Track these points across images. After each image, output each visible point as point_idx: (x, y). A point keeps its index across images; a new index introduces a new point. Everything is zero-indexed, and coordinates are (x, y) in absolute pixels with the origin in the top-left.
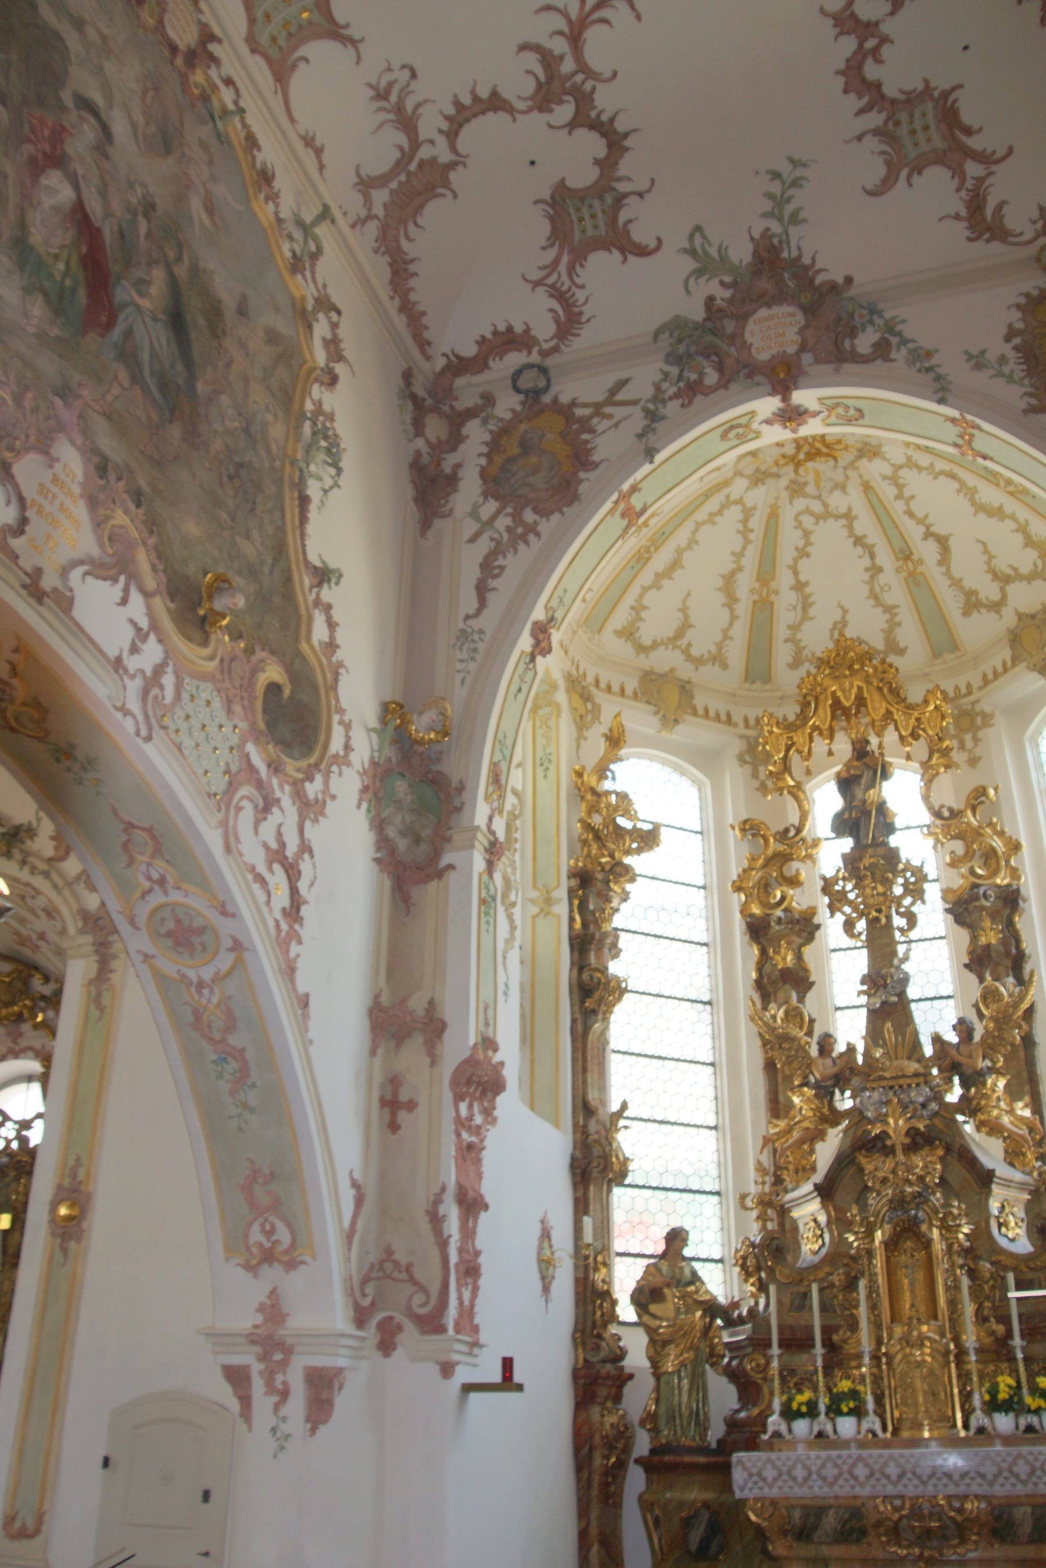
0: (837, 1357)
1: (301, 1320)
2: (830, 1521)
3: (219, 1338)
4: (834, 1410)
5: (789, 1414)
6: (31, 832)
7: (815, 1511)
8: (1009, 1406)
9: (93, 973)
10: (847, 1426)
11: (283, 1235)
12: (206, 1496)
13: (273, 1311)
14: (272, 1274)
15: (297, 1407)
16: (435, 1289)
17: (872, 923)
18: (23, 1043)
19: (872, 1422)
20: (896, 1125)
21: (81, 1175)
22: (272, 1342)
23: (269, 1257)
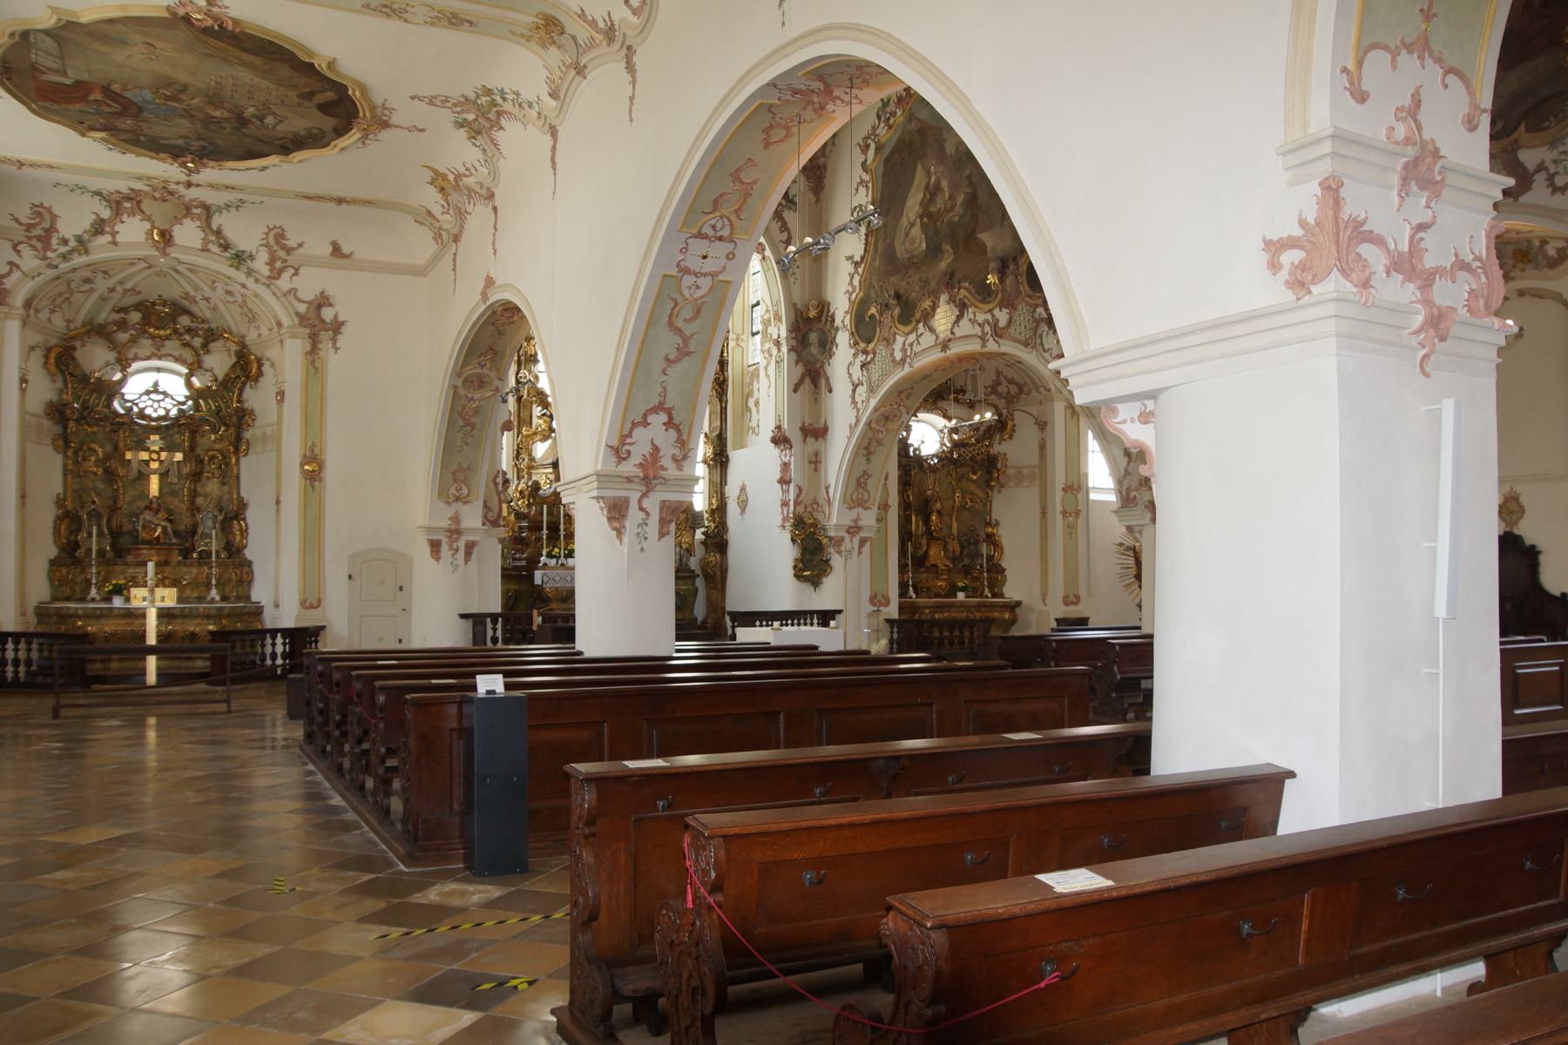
3: (429, 529)
5: (549, 555)
6: (251, 257)
9: (308, 348)
11: (465, 491)
13: (456, 519)
14: (458, 506)
15: (461, 555)
16: (496, 510)
18: (163, 351)
21: (317, 450)
22: (455, 532)
23: (457, 499)
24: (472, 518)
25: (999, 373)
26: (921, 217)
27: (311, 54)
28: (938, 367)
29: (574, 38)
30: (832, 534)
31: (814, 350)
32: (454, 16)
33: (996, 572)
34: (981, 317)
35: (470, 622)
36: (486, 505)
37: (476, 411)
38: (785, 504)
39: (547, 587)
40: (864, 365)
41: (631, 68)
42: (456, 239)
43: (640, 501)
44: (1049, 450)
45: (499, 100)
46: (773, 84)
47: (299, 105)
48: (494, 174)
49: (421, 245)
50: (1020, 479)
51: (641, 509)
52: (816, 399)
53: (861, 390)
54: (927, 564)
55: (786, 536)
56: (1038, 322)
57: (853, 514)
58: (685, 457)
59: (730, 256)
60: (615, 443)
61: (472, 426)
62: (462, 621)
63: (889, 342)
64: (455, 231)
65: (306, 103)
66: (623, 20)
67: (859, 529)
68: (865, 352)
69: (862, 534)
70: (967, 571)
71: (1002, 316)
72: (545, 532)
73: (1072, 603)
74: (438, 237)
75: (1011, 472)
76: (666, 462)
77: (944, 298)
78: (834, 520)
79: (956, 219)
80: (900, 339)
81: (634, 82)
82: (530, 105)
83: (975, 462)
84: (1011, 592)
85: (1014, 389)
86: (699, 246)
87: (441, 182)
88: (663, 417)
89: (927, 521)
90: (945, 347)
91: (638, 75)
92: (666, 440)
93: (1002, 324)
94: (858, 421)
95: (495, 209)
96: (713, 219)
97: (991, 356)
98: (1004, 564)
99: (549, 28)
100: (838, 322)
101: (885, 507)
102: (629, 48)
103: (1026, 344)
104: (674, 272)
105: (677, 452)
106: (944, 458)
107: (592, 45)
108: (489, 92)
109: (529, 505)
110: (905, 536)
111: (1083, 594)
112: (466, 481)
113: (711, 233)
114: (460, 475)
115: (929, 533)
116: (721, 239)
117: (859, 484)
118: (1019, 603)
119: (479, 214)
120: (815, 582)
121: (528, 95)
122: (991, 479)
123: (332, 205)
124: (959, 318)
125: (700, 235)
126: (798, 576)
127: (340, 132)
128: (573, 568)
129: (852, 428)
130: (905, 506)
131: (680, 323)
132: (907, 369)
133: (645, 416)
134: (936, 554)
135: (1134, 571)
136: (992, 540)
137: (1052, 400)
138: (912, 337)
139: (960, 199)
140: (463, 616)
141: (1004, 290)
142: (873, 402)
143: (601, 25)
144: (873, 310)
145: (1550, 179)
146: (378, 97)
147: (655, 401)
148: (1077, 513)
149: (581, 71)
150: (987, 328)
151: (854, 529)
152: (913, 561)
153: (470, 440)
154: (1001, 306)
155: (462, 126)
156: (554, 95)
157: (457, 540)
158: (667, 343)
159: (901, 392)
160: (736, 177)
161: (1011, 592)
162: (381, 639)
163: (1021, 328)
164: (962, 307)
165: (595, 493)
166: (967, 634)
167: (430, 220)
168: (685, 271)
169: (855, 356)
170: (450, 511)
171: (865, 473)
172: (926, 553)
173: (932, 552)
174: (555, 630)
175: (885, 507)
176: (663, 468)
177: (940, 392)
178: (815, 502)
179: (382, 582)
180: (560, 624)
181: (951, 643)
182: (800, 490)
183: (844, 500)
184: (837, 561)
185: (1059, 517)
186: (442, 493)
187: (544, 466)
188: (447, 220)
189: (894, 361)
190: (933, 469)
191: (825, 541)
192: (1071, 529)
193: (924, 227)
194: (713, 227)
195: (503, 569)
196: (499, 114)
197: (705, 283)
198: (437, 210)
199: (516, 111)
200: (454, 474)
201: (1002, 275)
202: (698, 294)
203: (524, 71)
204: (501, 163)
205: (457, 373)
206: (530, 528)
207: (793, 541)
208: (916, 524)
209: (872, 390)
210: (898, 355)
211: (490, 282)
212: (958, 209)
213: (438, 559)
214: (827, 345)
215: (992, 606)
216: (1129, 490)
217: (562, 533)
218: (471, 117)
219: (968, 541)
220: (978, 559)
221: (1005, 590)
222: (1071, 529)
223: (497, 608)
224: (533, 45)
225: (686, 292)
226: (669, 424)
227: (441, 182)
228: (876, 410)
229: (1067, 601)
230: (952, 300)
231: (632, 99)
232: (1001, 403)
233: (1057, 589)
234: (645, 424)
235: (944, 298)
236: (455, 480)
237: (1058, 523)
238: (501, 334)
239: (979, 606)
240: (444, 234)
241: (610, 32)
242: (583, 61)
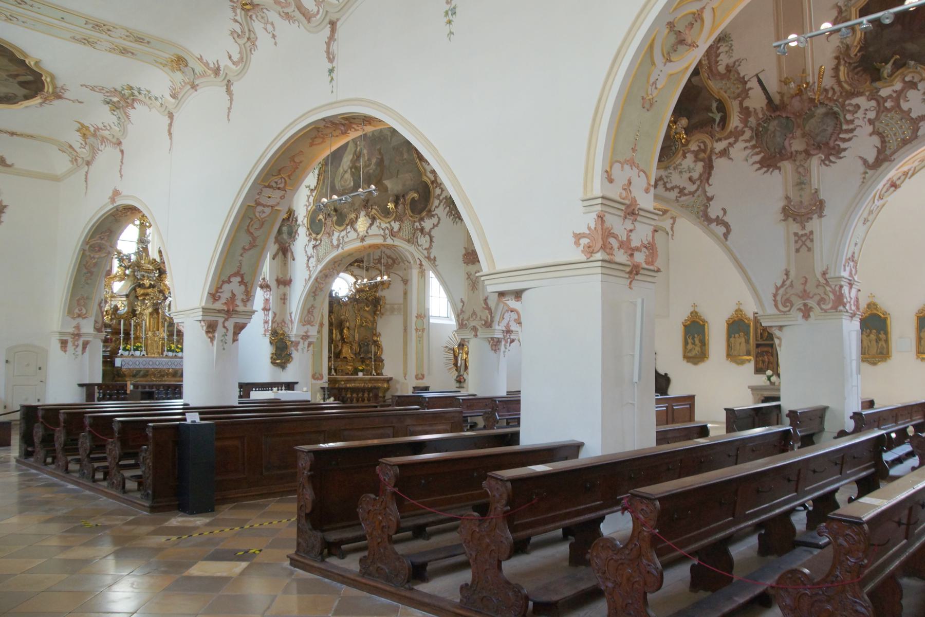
0: (137, 338)
1: (84, 330)
2: (142, 373)
3: (61, 333)
4: (135, 350)
5: (125, 349)
7: (138, 371)
8: (173, 351)
10: (138, 353)
11: (84, 311)
12: (40, 369)
13: (78, 327)
14: (80, 320)
15: (80, 348)
17: (142, 224)
19: (144, 352)
20: (147, 282)
23: (79, 316)
24: (88, 327)
26: (351, 169)
27: (26, 56)
28: (358, 250)
29: (193, 70)
30: (293, 339)
31: (285, 236)
32: (124, 49)
33: (379, 360)
34: (384, 225)
35: (85, 389)
36: (96, 322)
37: (95, 265)
38: (266, 322)
39: (124, 368)
40: (314, 247)
41: (229, 92)
42: (88, 163)
43: (223, 323)
45: (136, 93)
46: (323, 119)
47: (6, 80)
48: (124, 132)
49: (62, 164)
50: (392, 310)
51: (224, 327)
52: (285, 263)
53: (313, 261)
54: (342, 357)
55: (266, 341)
56: (416, 230)
57: (305, 328)
58: (248, 300)
59: (282, 197)
60: (213, 292)
61: (92, 273)
62: (80, 388)
63: (330, 235)
64: (89, 159)
65: (11, 80)
66: (226, 66)
67: (308, 337)
68: (316, 239)
69: (310, 340)
70: (363, 361)
71: (396, 226)
72: (122, 335)
74: (74, 160)
75: (388, 306)
76: (238, 302)
77: (363, 213)
78: (294, 332)
79: (371, 171)
80: (336, 234)
81: (231, 100)
82: (156, 99)
83: (369, 301)
84: (387, 372)
85: (390, 261)
86: (268, 192)
87: (83, 130)
88: (239, 279)
89: (341, 333)
90: (363, 240)
91: (234, 97)
92: (239, 290)
93: (396, 229)
94: (310, 277)
95: (122, 151)
96: (276, 179)
97: (389, 247)
98: (383, 357)
99: (180, 62)
100: (299, 222)
101: (321, 325)
102: (229, 81)
103: (409, 241)
104: (253, 204)
105: (244, 297)
106: (353, 299)
107: (203, 75)
108: (131, 88)
109: (112, 319)
110: (331, 341)
111: (425, 373)
112: (85, 305)
113: (274, 185)
114: (82, 302)
115: (343, 339)
116: (279, 188)
117: (309, 312)
118: (391, 379)
119: (107, 154)
120: (283, 366)
121: (155, 93)
122: (377, 310)
123: (7, 136)
124: (371, 225)
125: (270, 187)
126: (273, 363)
127: (26, 98)
128: (182, 358)
129: (306, 281)
130: (331, 324)
131: (252, 231)
132: (340, 250)
133: (229, 278)
134: (346, 352)
135: (453, 361)
136: (376, 343)
137: (411, 268)
138: (344, 233)
139: (374, 161)
140: (81, 385)
141: (397, 212)
142: (320, 267)
143: (212, 65)
144: (321, 217)
145: (665, 184)
146: (59, 84)
147: (235, 270)
148: (423, 330)
149: (194, 87)
150: (387, 232)
151: (305, 337)
152: (336, 355)
153: (89, 281)
154: (395, 220)
155: (108, 103)
156: (174, 96)
157: (77, 340)
158: (245, 240)
159: (335, 262)
160: (292, 159)
161: (387, 372)
162: (26, 400)
163: (405, 233)
164: (373, 219)
165: (200, 318)
166: (366, 395)
167: (71, 150)
168: (258, 204)
169: (309, 241)
170: (74, 323)
171: (312, 306)
172: (340, 352)
173: (344, 351)
174: (143, 393)
175: (321, 325)
176: (237, 306)
177: (354, 263)
178: (283, 321)
179: (28, 365)
180: (147, 390)
181: (358, 401)
182: (275, 314)
183: (300, 321)
184: (295, 355)
185: (414, 332)
186: (70, 312)
187: (121, 296)
188: (84, 152)
189: (332, 245)
190: (345, 304)
191: (289, 343)
192: (420, 339)
193: (353, 174)
194: (276, 183)
195: (104, 357)
196: (133, 100)
197: (268, 210)
198: (76, 146)
199: (147, 101)
200: (78, 301)
201: (396, 203)
202: (264, 215)
203: (157, 81)
204: (129, 126)
205: (86, 242)
206: (112, 333)
207: (271, 343)
208: (336, 335)
209: (319, 261)
210: (335, 243)
211: (116, 193)
212: (373, 166)
213: (65, 351)
214: (292, 234)
215: (378, 380)
216: (462, 320)
217: (132, 336)
218: (115, 99)
220: (369, 353)
222: (420, 339)
223: (99, 379)
224: (166, 69)
225: (257, 214)
226: (242, 282)
227: (83, 130)
228: (321, 271)
229: (417, 378)
230: (367, 215)
231: (230, 109)
233: (412, 371)
234: (229, 282)
235: (363, 213)
236: (79, 305)
237: (413, 335)
238: (117, 221)
239: (370, 380)
240: (80, 160)
241: (217, 71)
242: (197, 82)
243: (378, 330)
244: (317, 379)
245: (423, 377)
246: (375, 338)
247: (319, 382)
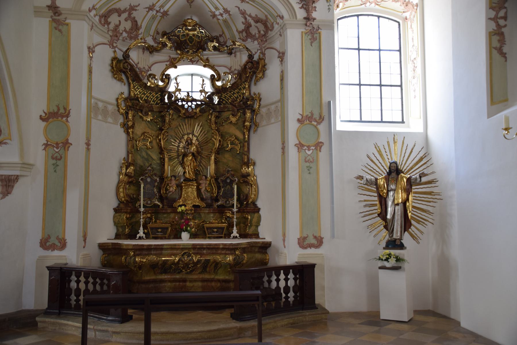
25: (243, 13)
44: (285, 79)
70: (221, 210)
73: (311, 246)
75: (263, 111)
98: (259, 204)
111: (325, 234)
135: (378, 209)
148: (319, 146)
190: (189, 116)
192: (309, 166)
219: (224, 181)
221: (260, 229)
222: (309, 166)
229: (303, 243)
232: (253, 46)
243: (252, 156)
244: (53, 247)
245: (319, 242)
246: (245, 170)
247: (56, 253)
